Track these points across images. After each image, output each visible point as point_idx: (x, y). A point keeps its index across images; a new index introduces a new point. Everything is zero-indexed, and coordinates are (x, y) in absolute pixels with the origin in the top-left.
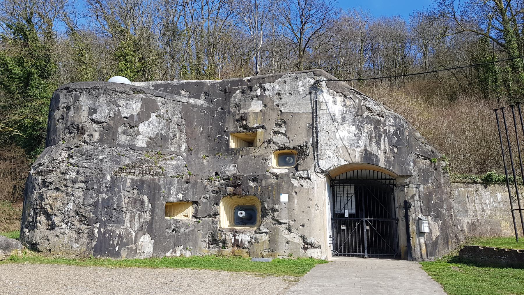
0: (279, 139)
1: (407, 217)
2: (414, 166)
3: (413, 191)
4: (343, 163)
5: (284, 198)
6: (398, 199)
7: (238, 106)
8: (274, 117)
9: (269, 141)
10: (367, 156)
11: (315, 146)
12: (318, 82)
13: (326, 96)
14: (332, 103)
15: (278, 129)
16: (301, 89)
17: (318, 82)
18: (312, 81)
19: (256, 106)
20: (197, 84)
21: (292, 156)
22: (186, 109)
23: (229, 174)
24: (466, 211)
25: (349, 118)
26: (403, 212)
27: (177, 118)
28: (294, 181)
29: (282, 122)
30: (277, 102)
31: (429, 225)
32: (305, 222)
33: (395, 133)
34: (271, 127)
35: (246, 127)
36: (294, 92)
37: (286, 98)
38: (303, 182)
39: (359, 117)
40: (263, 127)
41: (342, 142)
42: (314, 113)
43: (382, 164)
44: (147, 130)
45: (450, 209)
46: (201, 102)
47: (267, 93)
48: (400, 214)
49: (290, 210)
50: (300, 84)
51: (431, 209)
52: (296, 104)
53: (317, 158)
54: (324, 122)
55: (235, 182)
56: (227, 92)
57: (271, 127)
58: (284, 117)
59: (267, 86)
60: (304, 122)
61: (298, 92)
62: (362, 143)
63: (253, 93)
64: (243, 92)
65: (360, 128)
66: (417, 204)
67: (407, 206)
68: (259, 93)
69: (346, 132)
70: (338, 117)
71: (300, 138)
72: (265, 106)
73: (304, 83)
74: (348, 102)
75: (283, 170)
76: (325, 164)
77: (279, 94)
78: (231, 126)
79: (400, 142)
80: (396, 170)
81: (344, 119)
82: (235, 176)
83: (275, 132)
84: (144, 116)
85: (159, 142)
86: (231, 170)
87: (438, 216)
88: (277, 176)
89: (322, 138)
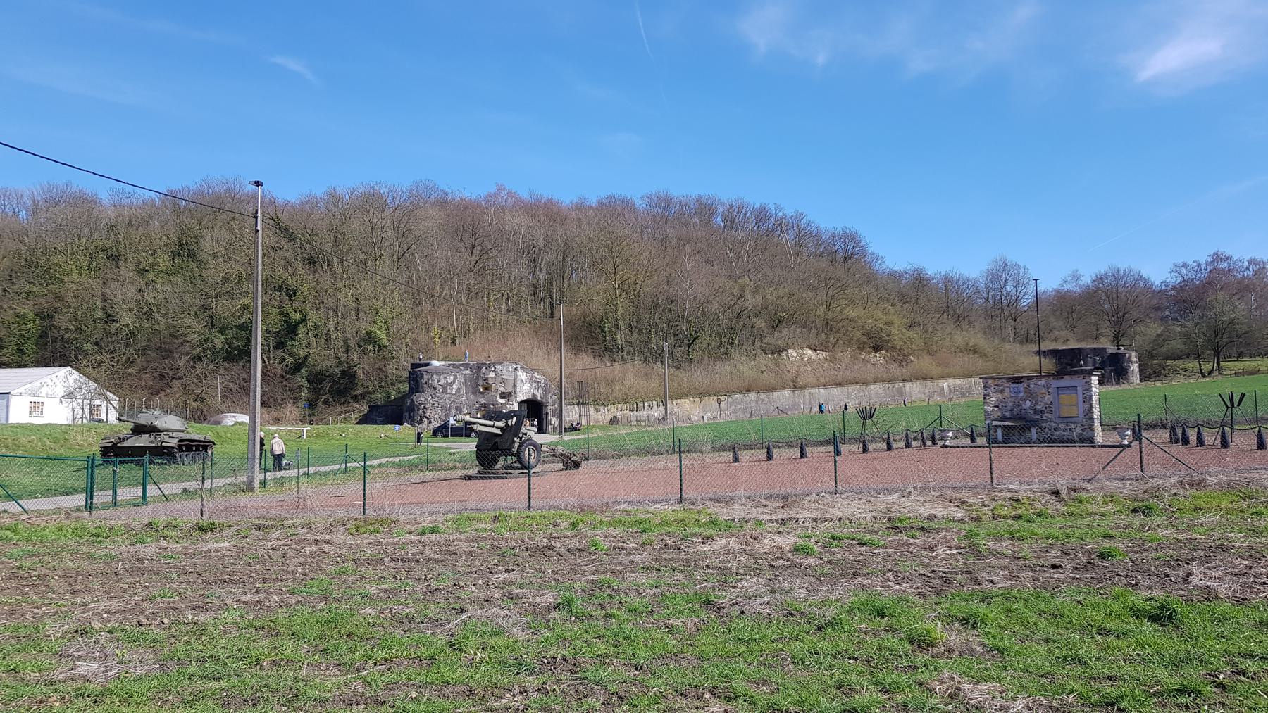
0: (502, 389)
2: (551, 398)
3: (549, 409)
10: (534, 395)
13: (519, 373)
14: (522, 375)
19: (492, 375)
29: (503, 381)
31: (554, 421)
41: (525, 391)
52: (507, 374)
54: (519, 382)
55: (485, 406)
56: (479, 368)
60: (511, 383)
69: (527, 387)
71: (510, 389)
75: (503, 401)
76: (519, 399)
79: (546, 390)
85: (458, 390)
86: (483, 401)
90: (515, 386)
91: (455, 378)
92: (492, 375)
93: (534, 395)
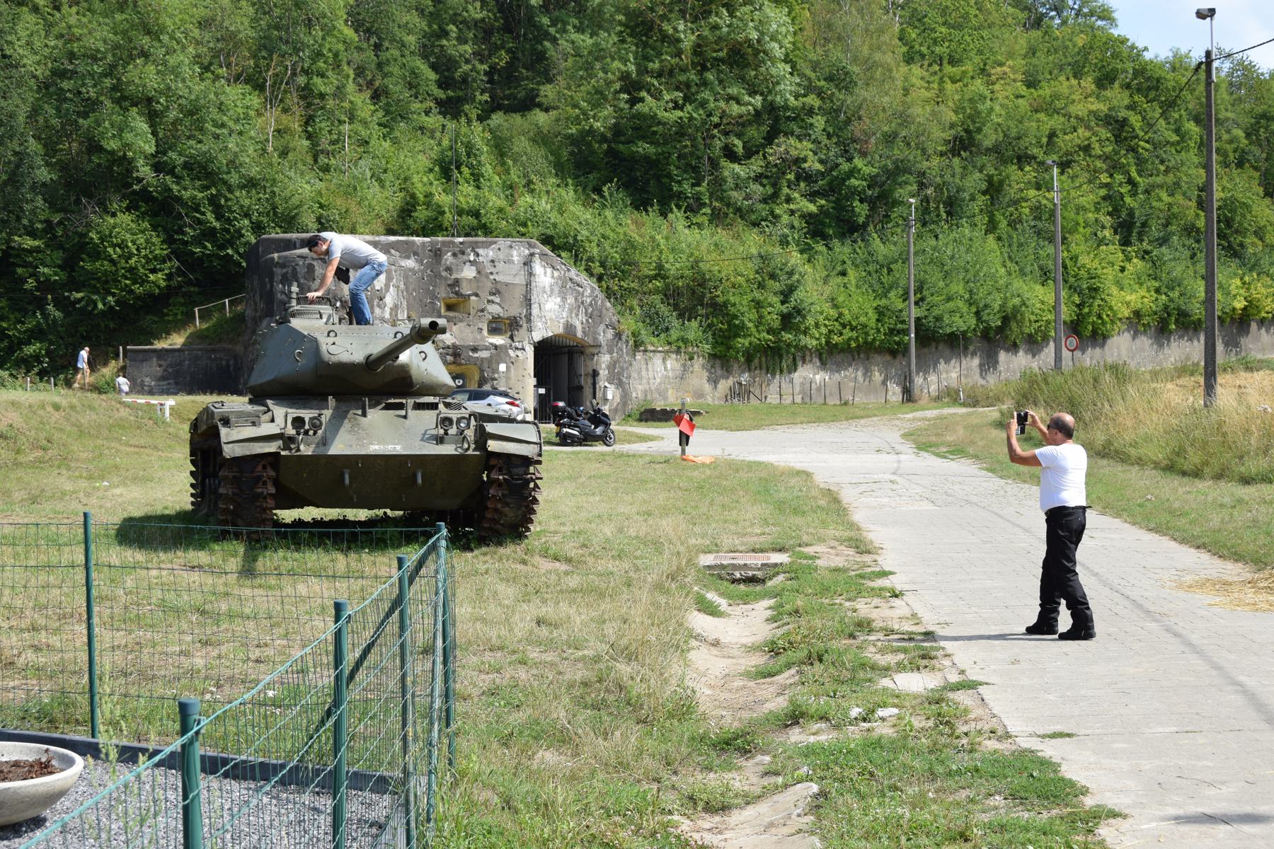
0: (494, 309)
1: (594, 384)
2: (605, 336)
3: (604, 360)
4: (550, 334)
5: (502, 367)
6: (583, 368)
7: (449, 269)
8: (489, 285)
9: (482, 311)
10: (569, 327)
11: (529, 318)
12: (532, 255)
13: (538, 267)
14: (544, 276)
15: (491, 298)
16: (516, 259)
17: (532, 255)
18: (527, 252)
20: (406, 242)
21: (507, 326)
22: (407, 273)
23: (449, 343)
24: (641, 378)
25: (556, 290)
26: (590, 381)
27: (402, 286)
28: (511, 352)
30: (492, 270)
32: (520, 389)
33: (591, 304)
34: (485, 295)
35: (457, 293)
36: (508, 261)
37: (500, 266)
38: (519, 353)
39: (564, 286)
40: (477, 295)
42: (528, 284)
43: (579, 334)
44: (389, 300)
45: (629, 377)
46: (410, 263)
47: (481, 259)
48: (586, 382)
49: (508, 378)
50: (515, 253)
51: (618, 379)
52: (510, 274)
53: (530, 330)
57: (485, 295)
58: (499, 286)
59: (481, 251)
60: (519, 294)
61: (513, 262)
62: (565, 315)
63: (465, 258)
64: (454, 255)
65: (564, 299)
66: (603, 373)
67: (595, 374)
68: (472, 258)
70: (548, 289)
71: (515, 310)
72: (479, 272)
73: (518, 253)
74: (556, 274)
75: (498, 340)
76: (537, 336)
77: (493, 261)
78: (443, 292)
80: (590, 340)
81: (552, 290)
82: (455, 347)
83: (489, 301)
84: (387, 286)
87: (620, 384)
88: (496, 347)
89: (535, 311)
90: (528, 302)
91: (389, 279)
92: (469, 273)
93: (569, 327)
